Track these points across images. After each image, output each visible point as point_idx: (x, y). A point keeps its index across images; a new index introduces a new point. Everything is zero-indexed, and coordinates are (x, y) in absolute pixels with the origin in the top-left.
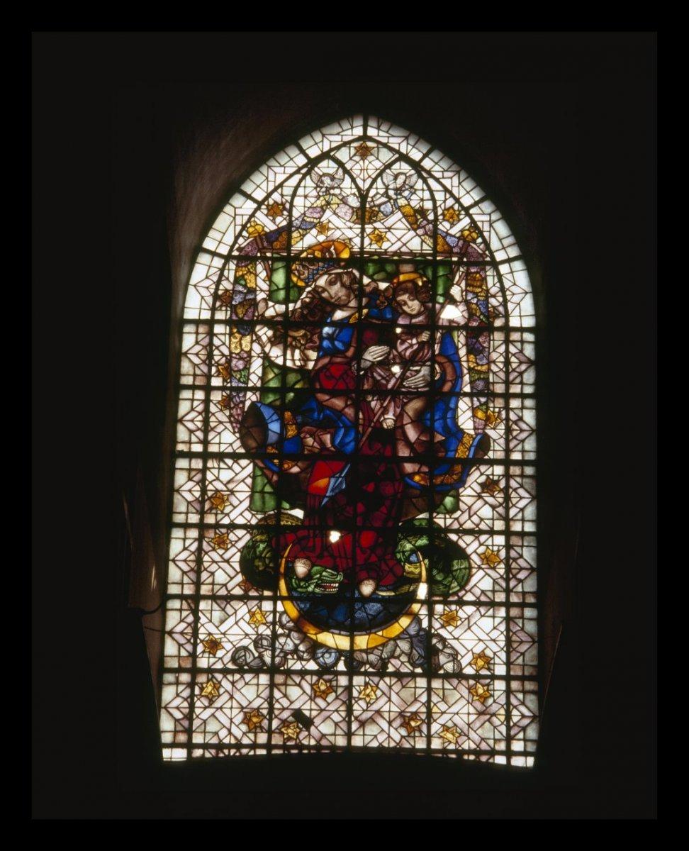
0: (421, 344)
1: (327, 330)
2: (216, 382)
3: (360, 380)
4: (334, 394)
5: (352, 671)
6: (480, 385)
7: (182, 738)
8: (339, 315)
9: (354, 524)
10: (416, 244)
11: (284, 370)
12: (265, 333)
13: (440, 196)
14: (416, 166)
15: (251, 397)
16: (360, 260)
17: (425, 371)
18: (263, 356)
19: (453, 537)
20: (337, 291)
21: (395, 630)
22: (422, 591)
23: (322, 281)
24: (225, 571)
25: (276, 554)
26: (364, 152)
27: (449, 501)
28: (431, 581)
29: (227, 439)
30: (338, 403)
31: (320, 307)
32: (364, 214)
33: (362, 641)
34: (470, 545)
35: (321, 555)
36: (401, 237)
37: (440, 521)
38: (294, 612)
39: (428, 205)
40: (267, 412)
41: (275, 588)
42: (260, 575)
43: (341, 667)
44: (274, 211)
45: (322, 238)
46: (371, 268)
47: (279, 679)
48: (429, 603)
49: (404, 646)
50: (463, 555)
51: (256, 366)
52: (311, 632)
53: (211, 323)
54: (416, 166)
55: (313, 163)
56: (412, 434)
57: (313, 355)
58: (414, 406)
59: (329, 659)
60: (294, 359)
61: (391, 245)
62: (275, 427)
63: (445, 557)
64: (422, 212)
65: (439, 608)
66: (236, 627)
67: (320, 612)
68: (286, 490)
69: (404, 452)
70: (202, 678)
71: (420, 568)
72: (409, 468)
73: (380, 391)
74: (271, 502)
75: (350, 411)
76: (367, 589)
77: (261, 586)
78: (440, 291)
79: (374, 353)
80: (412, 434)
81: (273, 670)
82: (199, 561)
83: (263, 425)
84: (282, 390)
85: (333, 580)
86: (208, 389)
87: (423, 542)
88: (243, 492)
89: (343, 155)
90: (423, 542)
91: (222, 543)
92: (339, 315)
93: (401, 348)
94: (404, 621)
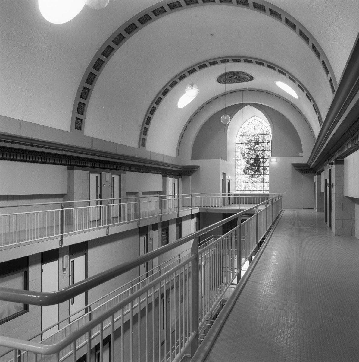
0: (262, 145)
1: (251, 144)
2: (239, 151)
3: (255, 149)
4: (252, 151)
5: (255, 183)
6: (268, 149)
7: (238, 190)
8: (253, 142)
9: (255, 166)
10: (261, 132)
11: (247, 149)
12: (245, 144)
13: (264, 126)
14: (261, 122)
15: (244, 152)
16: (255, 135)
17: (262, 148)
18: (244, 147)
19: (266, 167)
20: (252, 139)
21: (259, 178)
22: (262, 173)
23: (251, 138)
24: (242, 172)
25: (247, 170)
26: (255, 121)
27: (265, 163)
28: (263, 172)
29: (241, 157)
30: (253, 152)
31: (251, 141)
32: (255, 129)
33: (256, 179)
34: (267, 168)
35: (252, 169)
36: (259, 132)
37: (264, 165)
38: (249, 176)
39: (262, 127)
40: (245, 154)
41: (247, 174)
42: (245, 173)
43: (254, 182)
44: (245, 130)
45: (250, 132)
46: (256, 136)
47: (248, 183)
48: (263, 175)
49: (261, 179)
50: (267, 169)
51: (244, 148)
52: (250, 178)
53: (239, 143)
54: (261, 122)
55: (249, 123)
56: (261, 155)
57: (250, 147)
58: (262, 152)
59: (253, 181)
60: (248, 147)
61: (258, 133)
62: (246, 155)
63: (265, 169)
64: (261, 128)
65: (264, 175)
66: (244, 178)
67: (252, 176)
68: (248, 162)
69: (260, 157)
70: (240, 184)
71: (262, 171)
72: (261, 159)
73: (257, 151)
74: (246, 164)
75: (254, 153)
76: (257, 173)
77: (246, 173)
78: (264, 138)
79: (257, 146)
80: (261, 155)
81: (247, 183)
82: (239, 171)
83: (245, 155)
84: (247, 151)
85: (253, 173)
86: (239, 151)
87: (262, 168)
88: (243, 163)
89: (252, 122)
90: (262, 168)
91: (241, 169)
92: (253, 142)
93: (259, 145)
94: (260, 177)
